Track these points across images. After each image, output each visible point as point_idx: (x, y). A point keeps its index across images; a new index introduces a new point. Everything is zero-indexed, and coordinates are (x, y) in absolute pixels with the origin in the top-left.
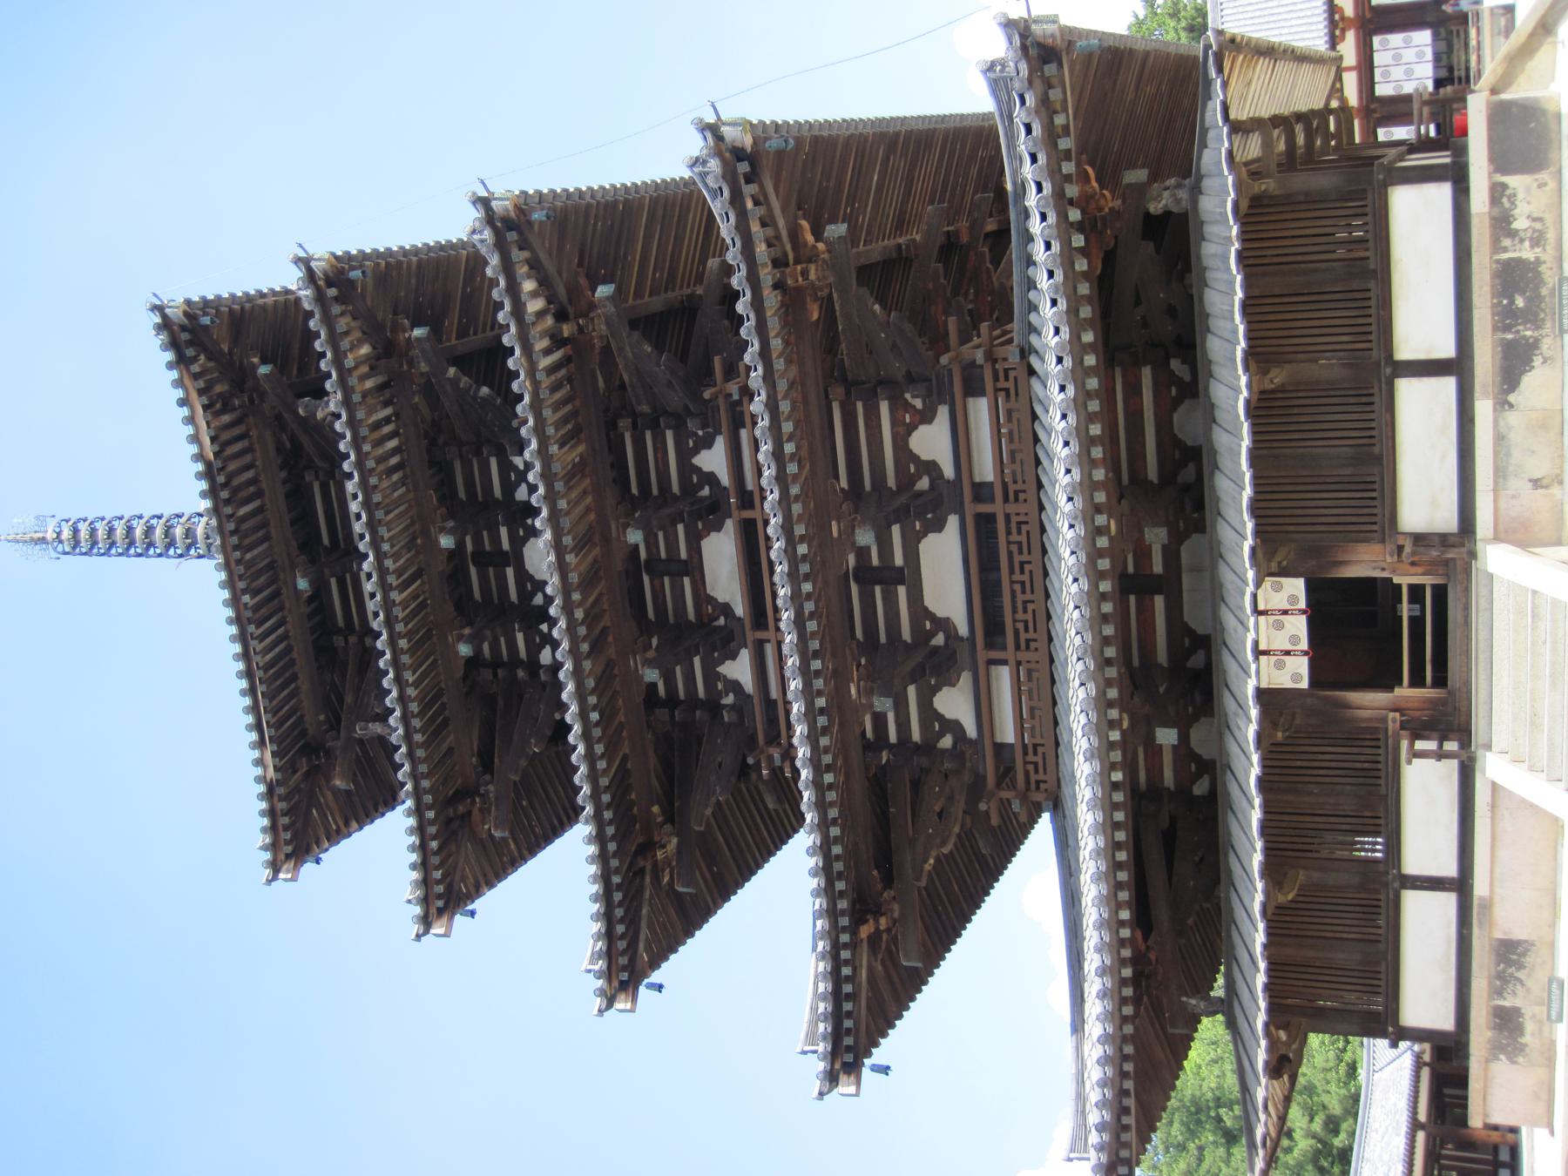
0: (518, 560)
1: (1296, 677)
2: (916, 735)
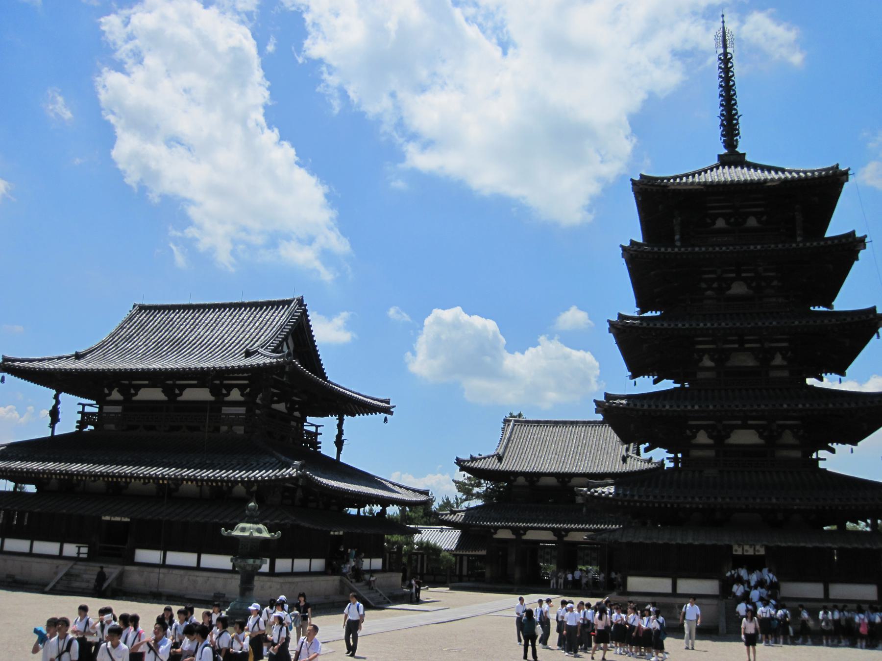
1: (736, 551)
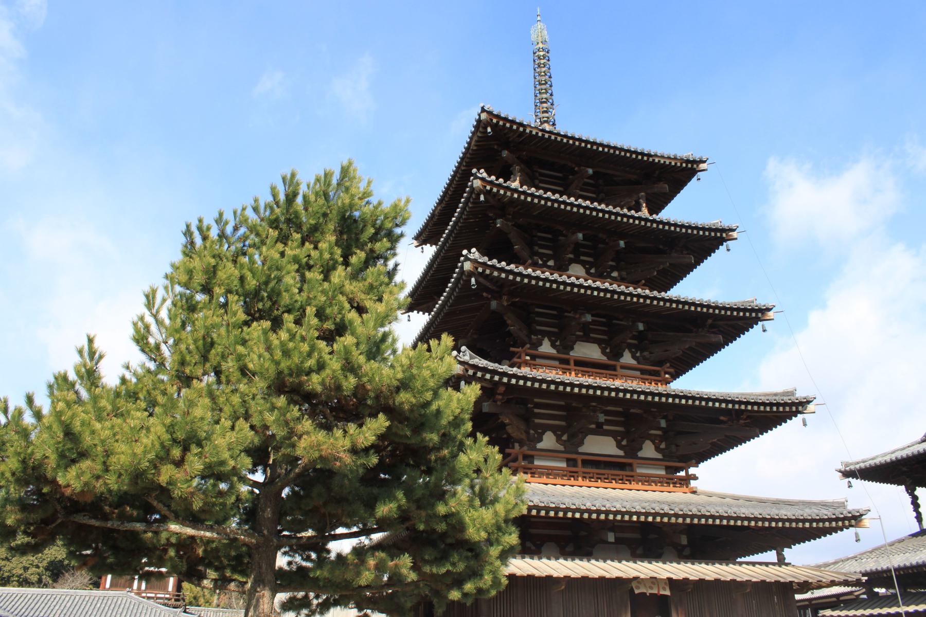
0: (577, 261)
2: (537, 421)
